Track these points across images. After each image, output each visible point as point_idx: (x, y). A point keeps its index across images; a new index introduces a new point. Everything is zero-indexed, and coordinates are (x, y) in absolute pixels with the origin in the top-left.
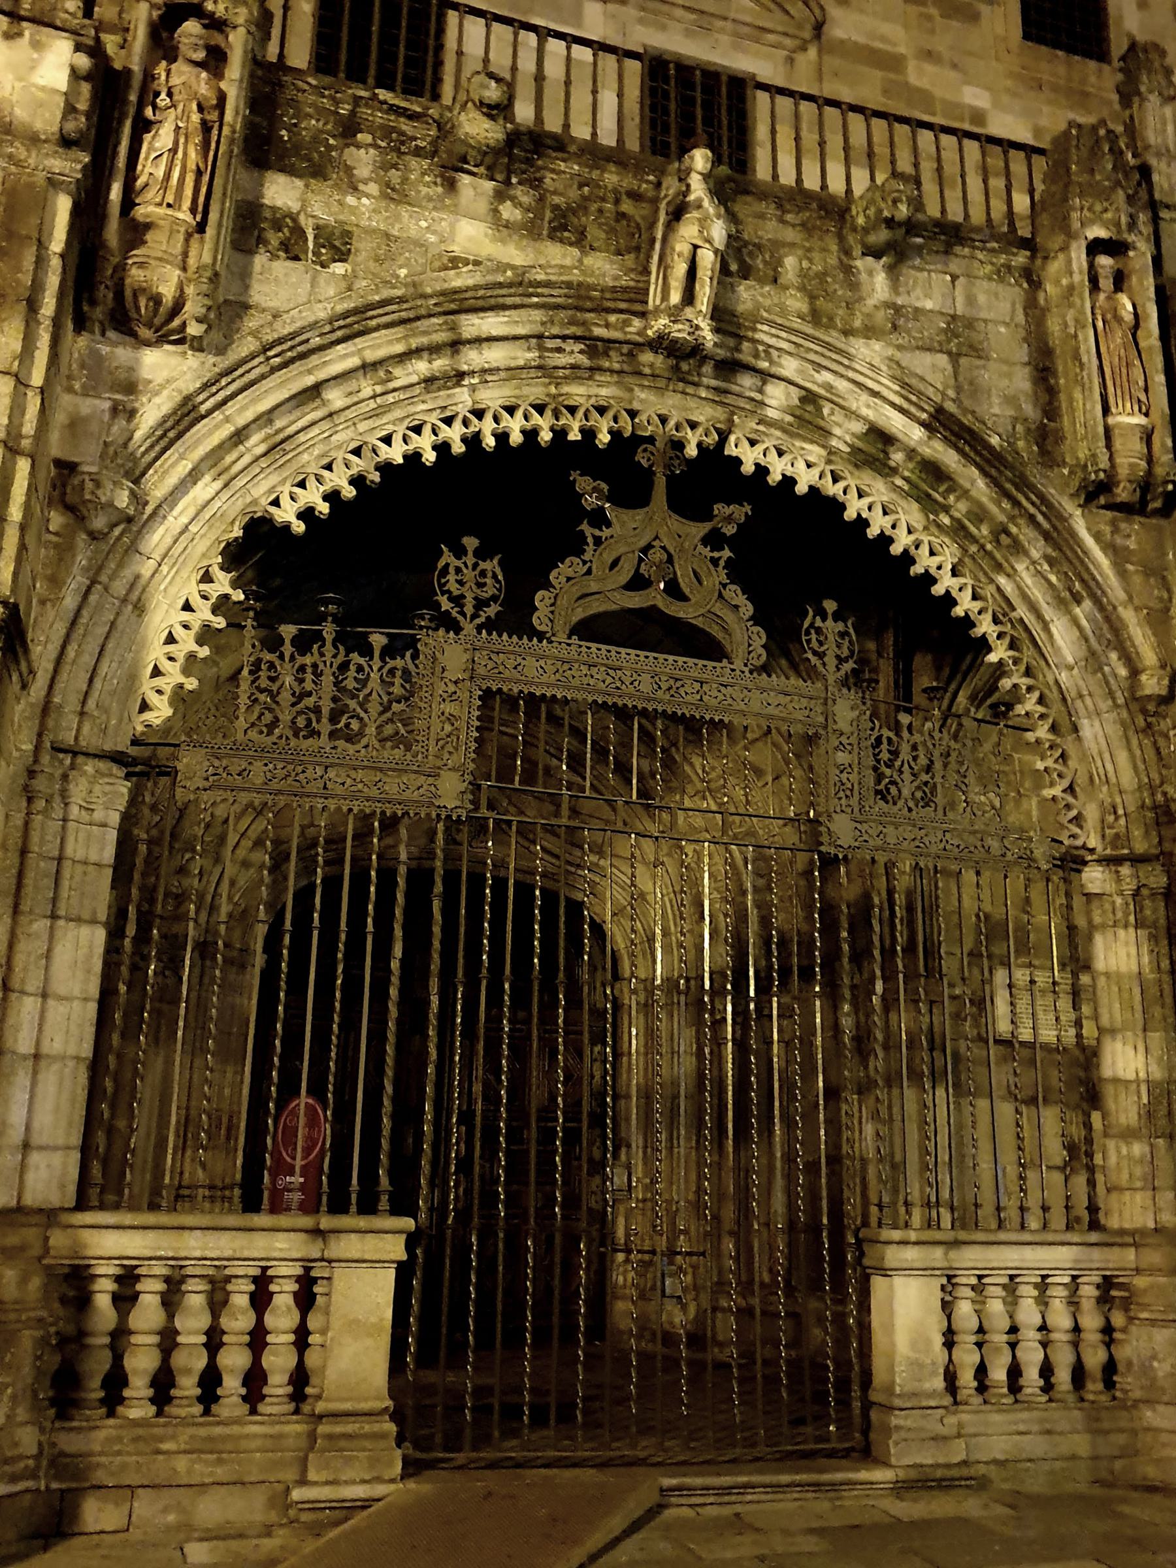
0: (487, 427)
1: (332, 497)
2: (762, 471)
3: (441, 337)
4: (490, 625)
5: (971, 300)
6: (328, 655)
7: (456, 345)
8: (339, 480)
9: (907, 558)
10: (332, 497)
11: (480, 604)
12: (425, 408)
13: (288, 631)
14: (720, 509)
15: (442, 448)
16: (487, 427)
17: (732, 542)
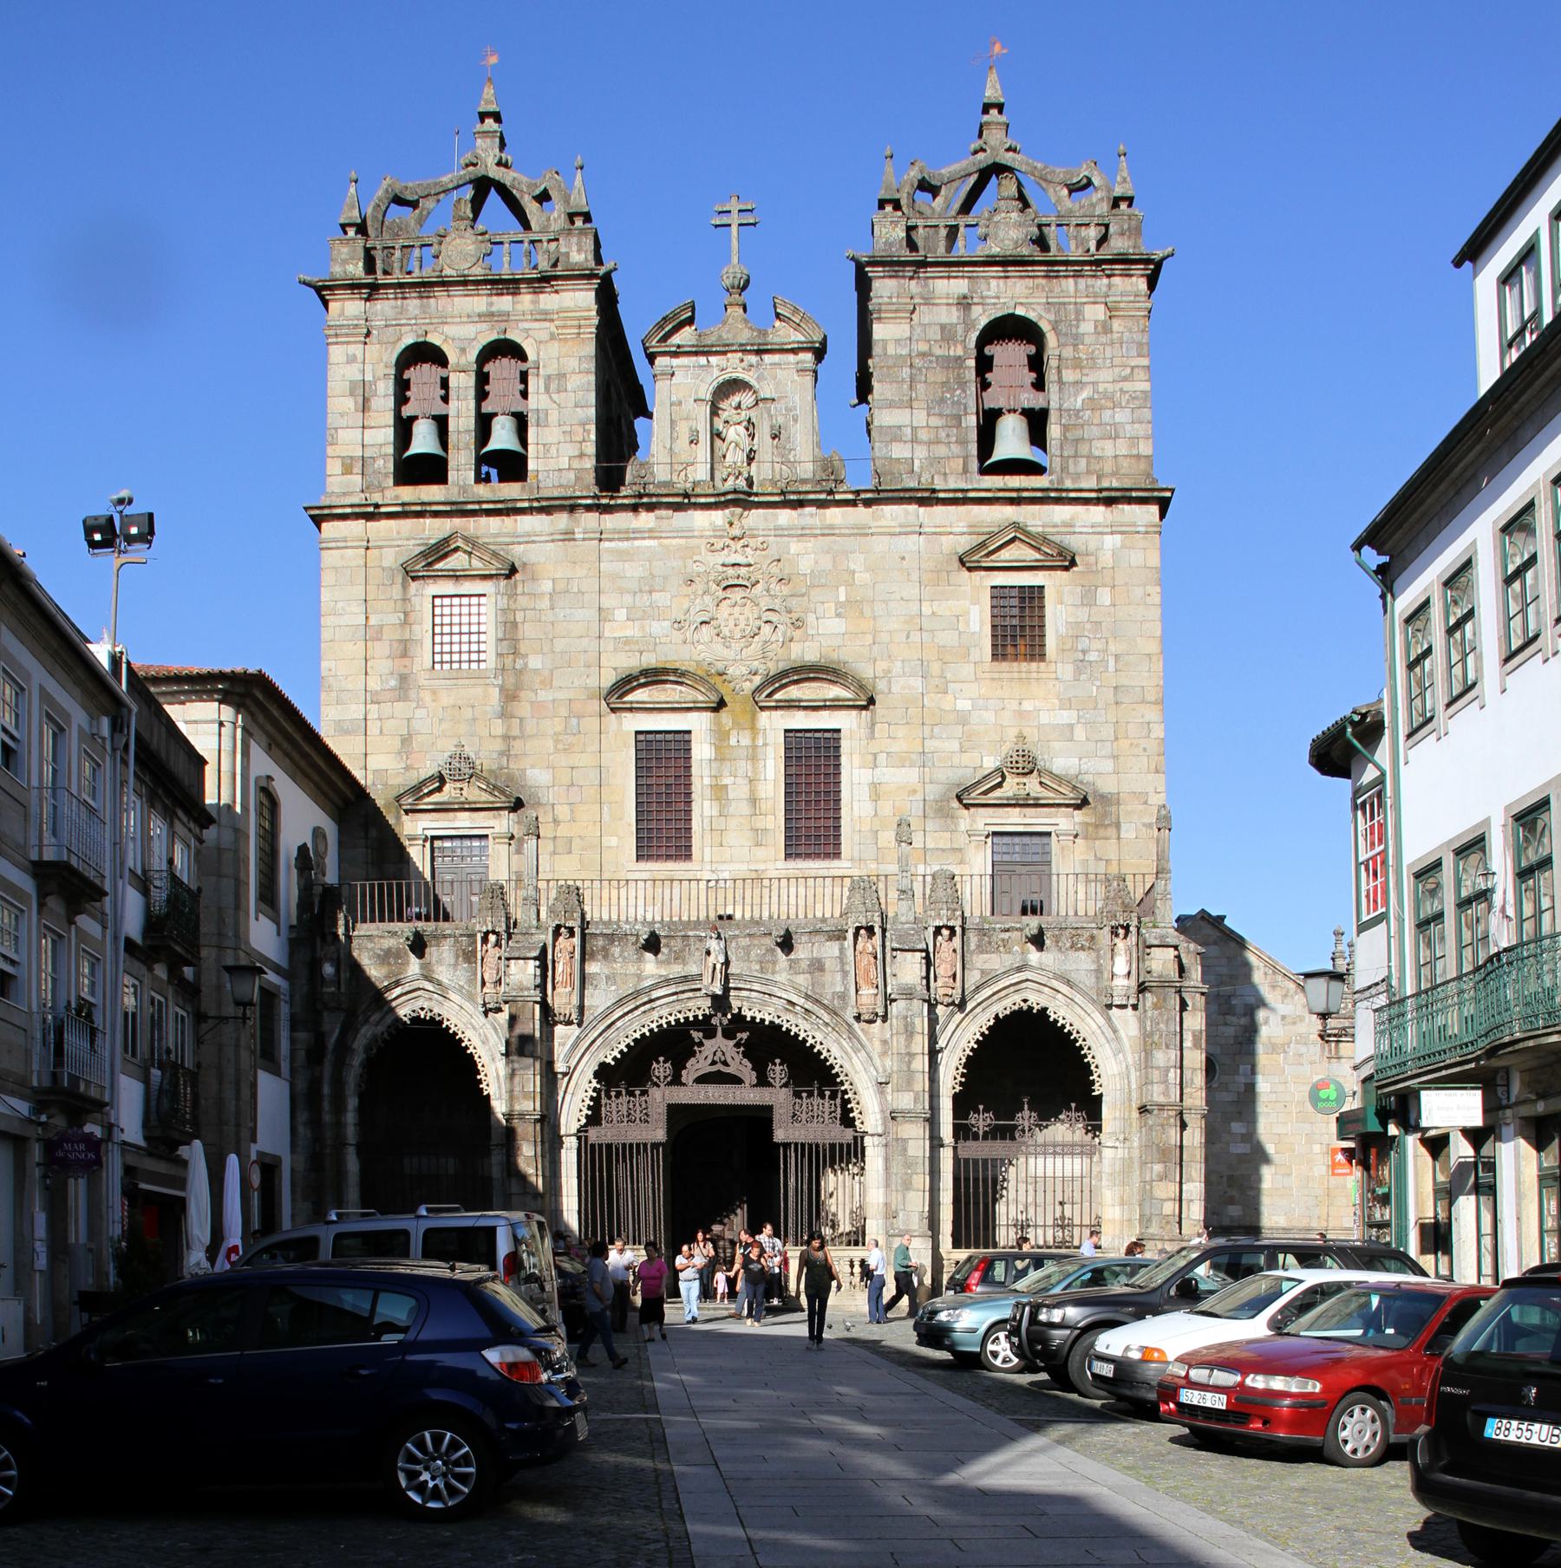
0: (664, 1021)
1: (621, 1052)
2: (753, 1018)
3: (646, 999)
4: (669, 1084)
5: (819, 950)
6: (624, 1099)
7: (651, 1001)
8: (623, 1047)
9: (805, 1041)
10: (621, 1052)
11: (665, 1077)
12: (646, 1020)
13: (613, 1094)
14: (739, 1035)
15: (651, 1031)
16: (664, 1021)
17: (744, 1045)
